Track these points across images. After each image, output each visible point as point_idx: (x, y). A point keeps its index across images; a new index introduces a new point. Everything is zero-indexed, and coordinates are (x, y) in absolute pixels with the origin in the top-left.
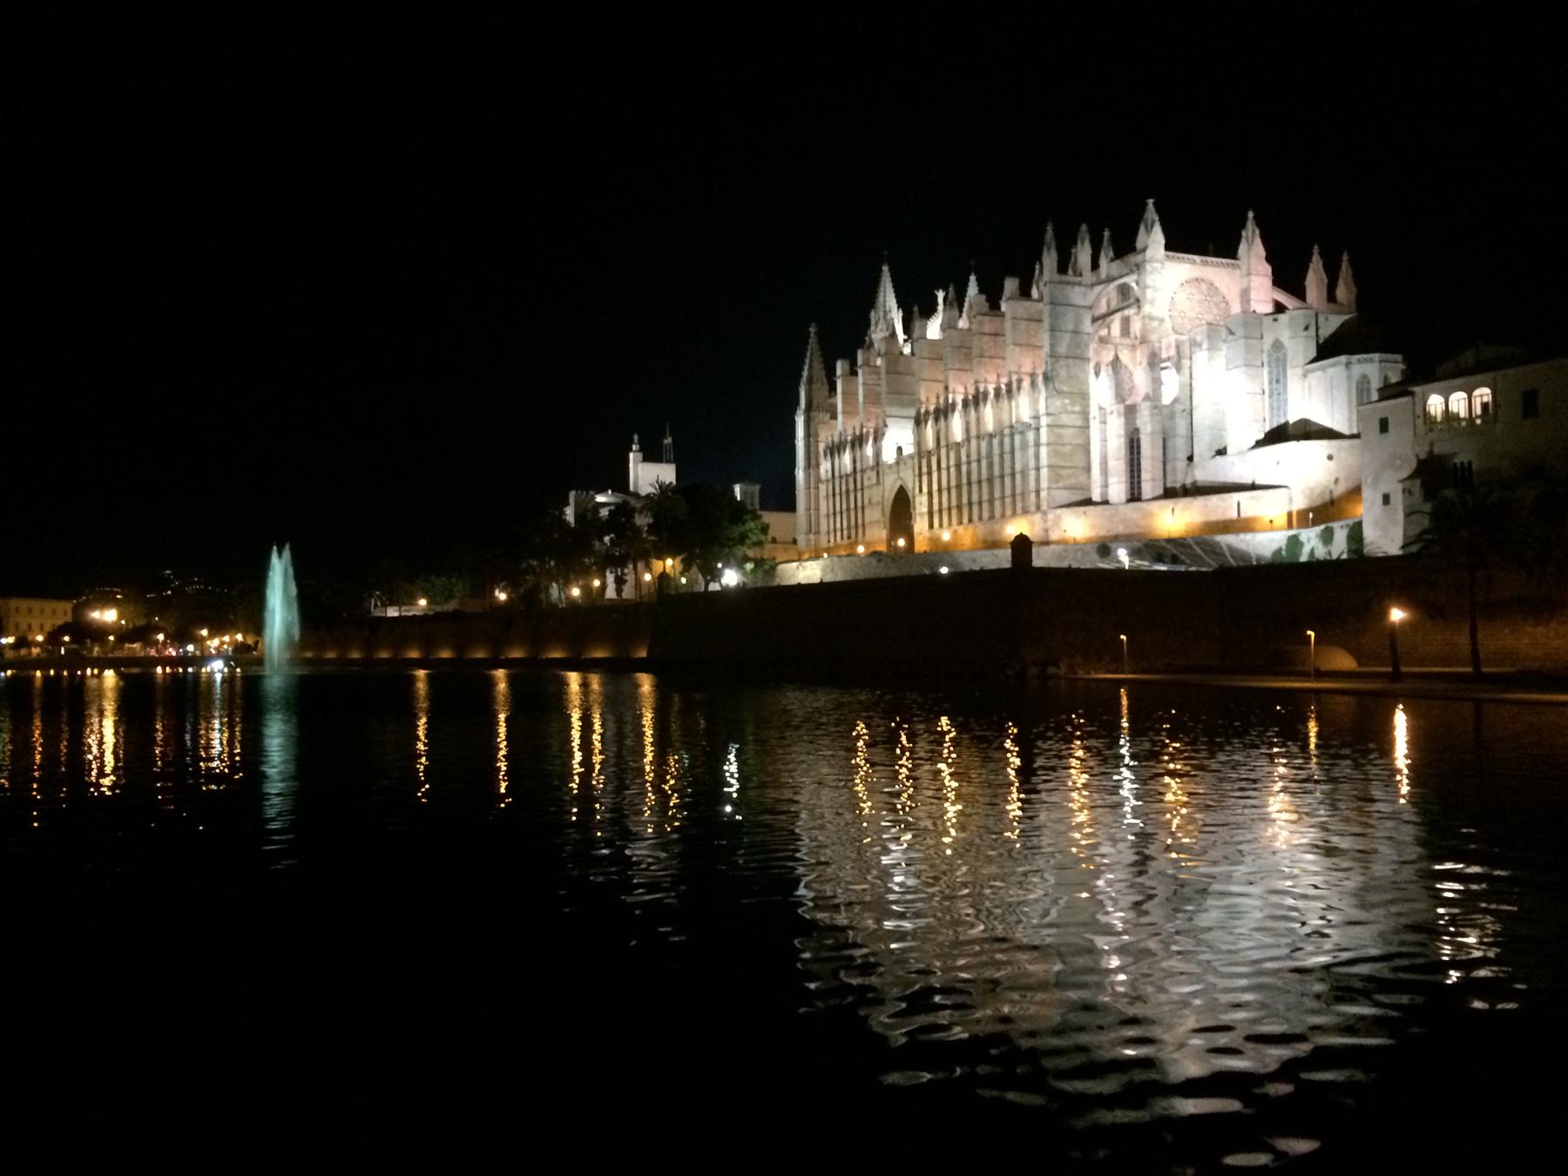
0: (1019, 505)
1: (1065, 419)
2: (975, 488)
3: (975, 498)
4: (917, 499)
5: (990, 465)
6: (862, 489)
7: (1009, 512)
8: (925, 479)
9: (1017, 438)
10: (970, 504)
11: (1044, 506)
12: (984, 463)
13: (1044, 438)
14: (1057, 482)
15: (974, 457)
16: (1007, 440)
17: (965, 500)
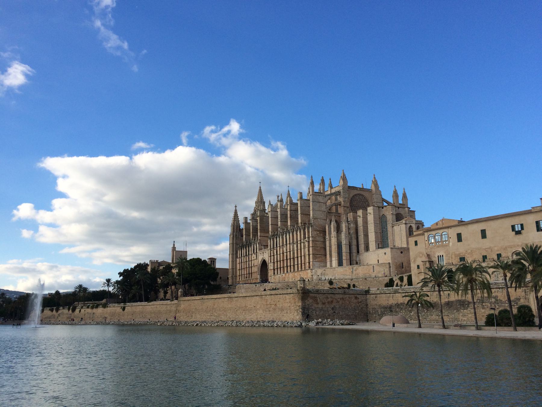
0: (303, 267)
1: (318, 239)
2: (289, 261)
3: (289, 264)
4: (270, 264)
5: (294, 253)
6: (251, 261)
7: (300, 269)
8: (272, 257)
9: (302, 244)
10: (287, 267)
11: (311, 268)
12: (292, 253)
13: (311, 245)
14: (315, 260)
15: (288, 250)
16: (299, 245)
17: (285, 265)
